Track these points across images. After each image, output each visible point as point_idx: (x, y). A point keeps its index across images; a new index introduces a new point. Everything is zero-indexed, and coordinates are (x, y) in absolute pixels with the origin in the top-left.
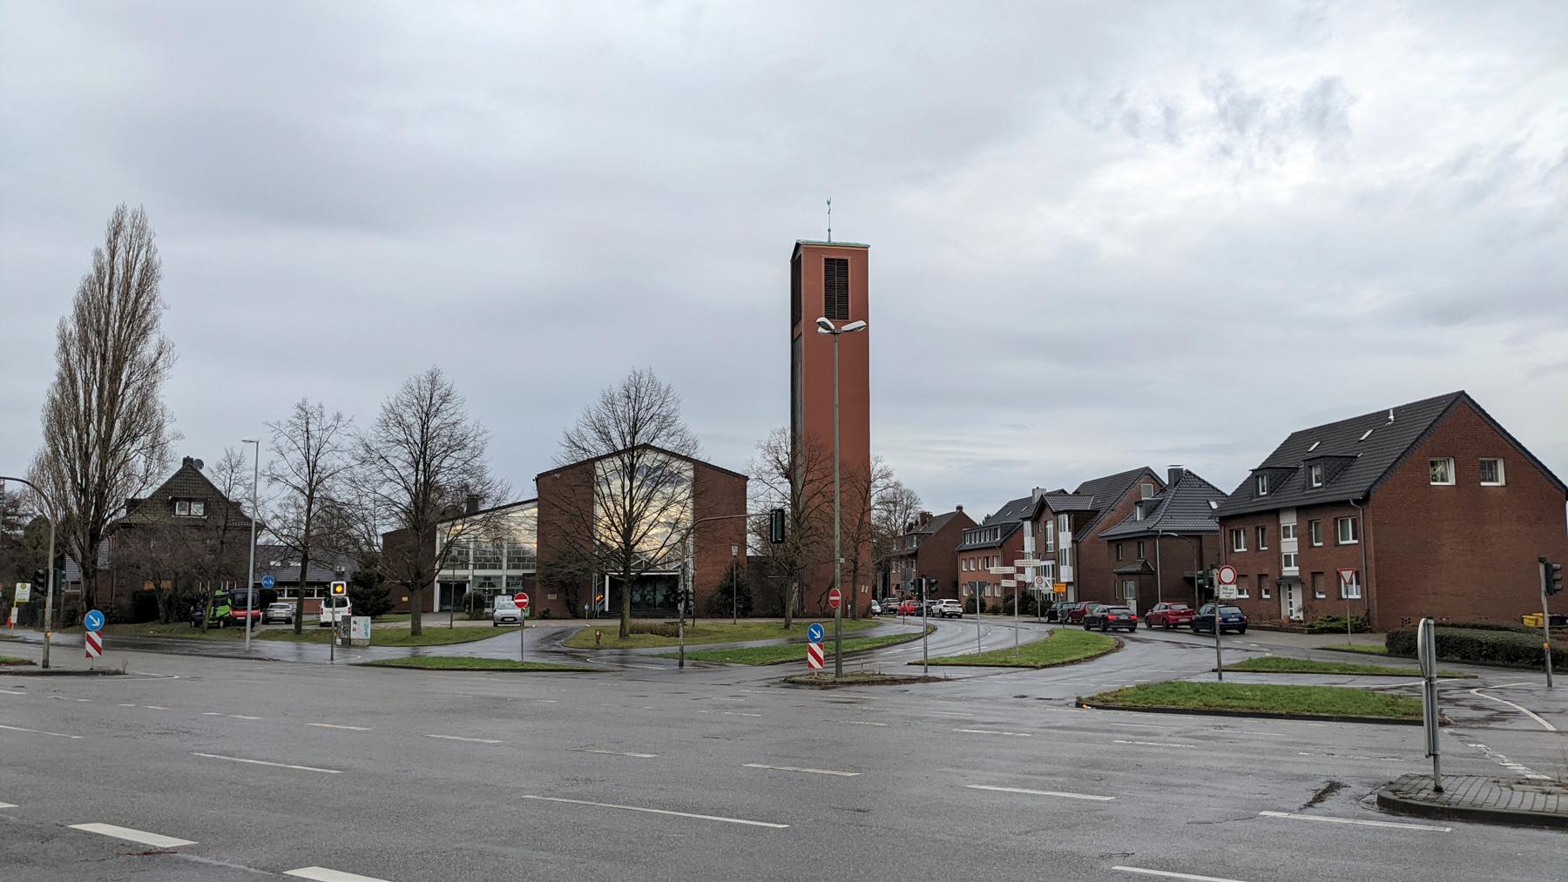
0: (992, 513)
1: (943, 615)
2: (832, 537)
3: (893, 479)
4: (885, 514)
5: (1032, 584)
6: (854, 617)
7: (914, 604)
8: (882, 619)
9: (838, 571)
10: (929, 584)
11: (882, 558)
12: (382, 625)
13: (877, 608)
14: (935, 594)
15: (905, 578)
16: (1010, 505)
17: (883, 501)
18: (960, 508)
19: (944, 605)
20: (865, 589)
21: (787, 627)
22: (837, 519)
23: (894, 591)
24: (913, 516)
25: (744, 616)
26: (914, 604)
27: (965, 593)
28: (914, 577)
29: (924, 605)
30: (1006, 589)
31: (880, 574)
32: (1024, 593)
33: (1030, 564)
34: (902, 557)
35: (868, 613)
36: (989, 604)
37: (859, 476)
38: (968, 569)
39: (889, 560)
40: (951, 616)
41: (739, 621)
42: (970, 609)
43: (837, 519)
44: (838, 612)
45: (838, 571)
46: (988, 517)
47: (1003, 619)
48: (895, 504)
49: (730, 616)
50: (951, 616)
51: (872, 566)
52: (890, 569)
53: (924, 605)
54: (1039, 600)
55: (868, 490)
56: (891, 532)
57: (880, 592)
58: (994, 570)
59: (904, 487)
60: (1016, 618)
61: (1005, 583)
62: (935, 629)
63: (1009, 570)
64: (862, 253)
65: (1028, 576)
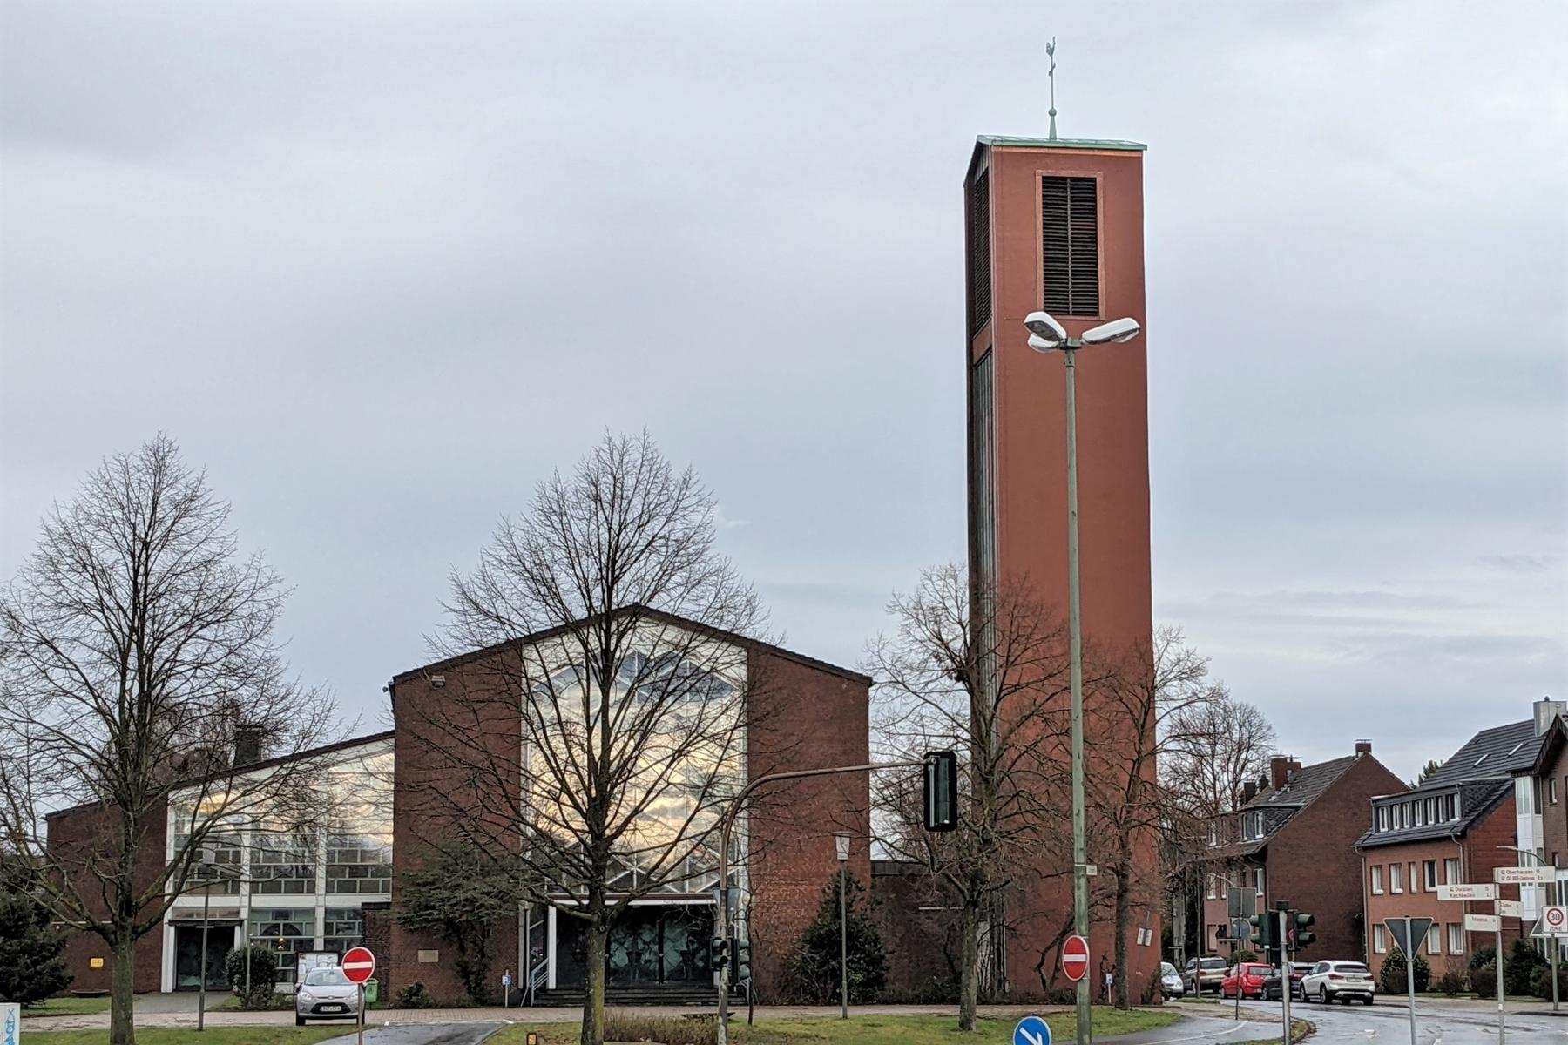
0: (1441, 759)
1: (1329, 998)
2: (1068, 816)
3: (1207, 682)
4: (1189, 762)
5: (1537, 925)
6: (1120, 1003)
7: (1257, 971)
8: (1186, 1006)
9: (1081, 895)
10: (1297, 926)
11: (1184, 863)
12: (45, 1023)
13: (1174, 982)
14: (1309, 948)
15: (1239, 911)
16: (1485, 740)
17: (1185, 733)
18: (1364, 748)
19: (1330, 974)
20: (1145, 937)
21: (965, 1025)
22: (1078, 775)
23: (1213, 942)
24: (1255, 767)
25: (866, 1000)
26: (1257, 971)
27: (1380, 945)
28: (1259, 909)
29: (1284, 973)
30: (1476, 937)
31: (1179, 903)
32: (1519, 947)
33: (1532, 877)
34: (1230, 862)
35: (1154, 993)
36: (1437, 970)
37: (1129, 676)
38: (1386, 888)
39: (1199, 868)
40: (1348, 999)
41: (855, 1012)
42: (1391, 984)
43: (1078, 775)
44: (1083, 990)
45: (1081, 895)
46: (1431, 770)
47: (1470, 1007)
48: (1213, 737)
49: (833, 1000)
50: (1348, 999)
51: (1159, 882)
52: (1203, 890)
53: (1284, 973)
54: (1553, 961)
55: (1149, 707)
56: (1204, 804)
57: (1179, 943)
58: (1451, 890)
59: (1234, 698)
60: (1501, 1004)
61: (1473, 923)
62: (1310, 1030)
63: (1482, 892)
64: (1127, 162)
65: (1529, 907)
